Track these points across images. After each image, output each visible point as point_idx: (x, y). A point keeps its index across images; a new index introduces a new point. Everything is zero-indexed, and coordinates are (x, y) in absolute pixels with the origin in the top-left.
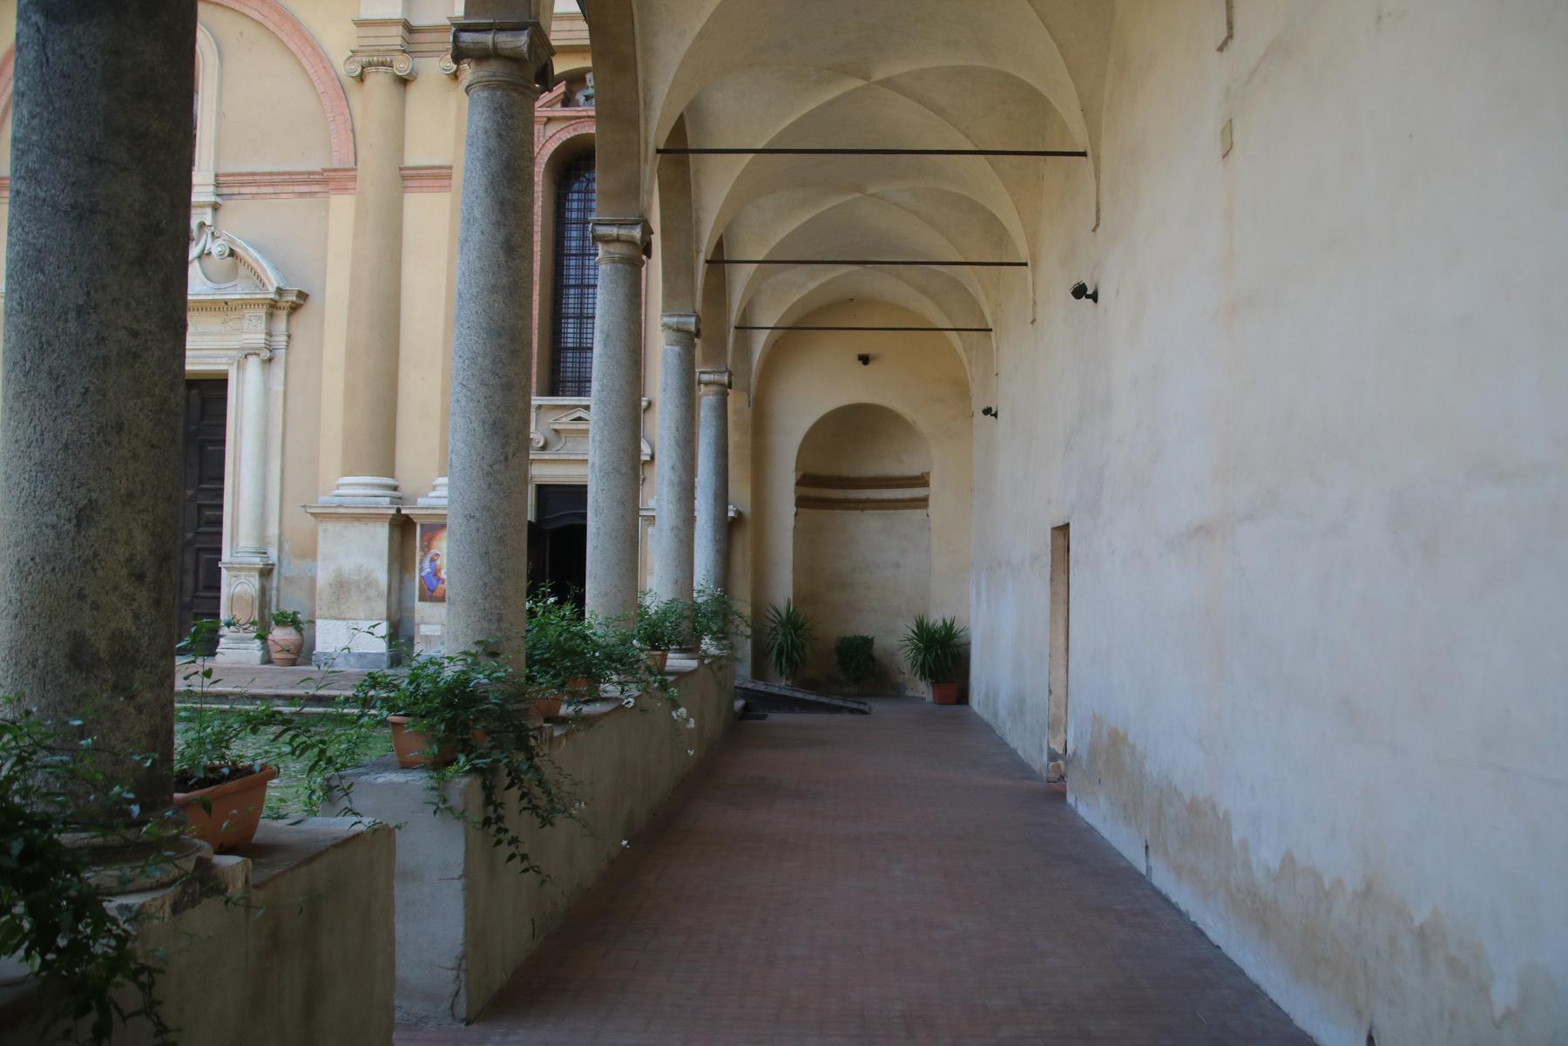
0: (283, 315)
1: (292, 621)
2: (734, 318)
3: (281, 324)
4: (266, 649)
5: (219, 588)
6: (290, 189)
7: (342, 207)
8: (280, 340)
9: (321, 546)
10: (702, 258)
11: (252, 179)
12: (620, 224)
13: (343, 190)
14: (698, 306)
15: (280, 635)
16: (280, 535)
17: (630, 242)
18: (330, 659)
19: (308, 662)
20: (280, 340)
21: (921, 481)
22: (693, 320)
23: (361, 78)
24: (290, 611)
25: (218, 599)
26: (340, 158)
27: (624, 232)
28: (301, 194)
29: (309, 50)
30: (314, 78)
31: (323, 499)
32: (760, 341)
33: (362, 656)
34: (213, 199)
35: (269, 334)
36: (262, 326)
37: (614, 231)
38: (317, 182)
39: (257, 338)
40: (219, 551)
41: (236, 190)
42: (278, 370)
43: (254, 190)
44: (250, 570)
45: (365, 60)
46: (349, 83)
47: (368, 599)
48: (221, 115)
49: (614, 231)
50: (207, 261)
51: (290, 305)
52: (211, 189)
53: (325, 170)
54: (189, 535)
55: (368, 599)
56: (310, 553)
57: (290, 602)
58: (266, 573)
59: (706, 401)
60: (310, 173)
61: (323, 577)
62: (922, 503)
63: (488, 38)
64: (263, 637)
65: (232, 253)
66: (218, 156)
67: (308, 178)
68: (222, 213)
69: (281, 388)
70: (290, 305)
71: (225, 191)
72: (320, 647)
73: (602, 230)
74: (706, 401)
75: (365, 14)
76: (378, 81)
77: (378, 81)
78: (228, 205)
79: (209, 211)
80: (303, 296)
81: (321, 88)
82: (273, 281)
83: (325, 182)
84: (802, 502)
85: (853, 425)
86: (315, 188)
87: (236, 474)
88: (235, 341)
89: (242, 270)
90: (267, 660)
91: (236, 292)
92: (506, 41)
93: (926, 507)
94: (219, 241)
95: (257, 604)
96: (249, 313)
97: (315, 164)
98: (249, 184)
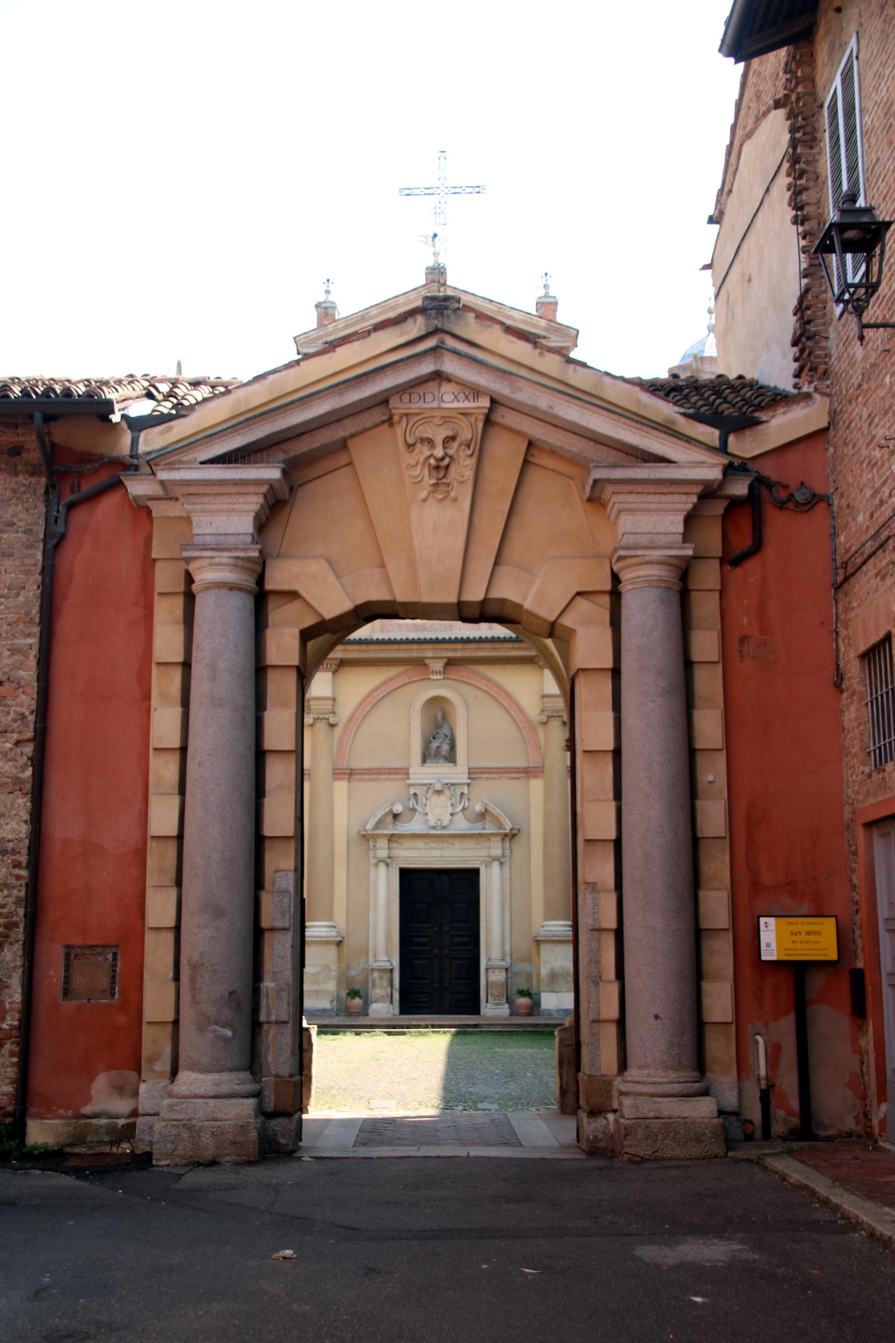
0: (507, 840)
1: (522, 993)
3: (507, 844)
6: (507, 775)
7: (537, 786)
8: (508, 852)
11: (487, 770)
13: (536, 777)
15: (523, 1001)
18: (549, 1013)
23: (544, 724)
28: (513, 778)
29: (514, 707)
30: (517, 720)
33: (566, 1010)
42: (507, 868)
43: (488, 776)
47: (568, 982)
48: (469, 738)
52: (467, 776)
53: (526, 768)
55: (568, 982)
60: (518, 768)
61: (544, 971)
67: (516, 770)
69: (508, 876)
71: (472, 776)
72: (544, 1006)
78: (476, 782)
79: (466, 787)
80: (519, 830)
81: (521, 726)
82: (508, 826)
86: (520, 775)
88: (484, 853)
90: (511, 1015)
96: (493, 839)
97: (521, 763)
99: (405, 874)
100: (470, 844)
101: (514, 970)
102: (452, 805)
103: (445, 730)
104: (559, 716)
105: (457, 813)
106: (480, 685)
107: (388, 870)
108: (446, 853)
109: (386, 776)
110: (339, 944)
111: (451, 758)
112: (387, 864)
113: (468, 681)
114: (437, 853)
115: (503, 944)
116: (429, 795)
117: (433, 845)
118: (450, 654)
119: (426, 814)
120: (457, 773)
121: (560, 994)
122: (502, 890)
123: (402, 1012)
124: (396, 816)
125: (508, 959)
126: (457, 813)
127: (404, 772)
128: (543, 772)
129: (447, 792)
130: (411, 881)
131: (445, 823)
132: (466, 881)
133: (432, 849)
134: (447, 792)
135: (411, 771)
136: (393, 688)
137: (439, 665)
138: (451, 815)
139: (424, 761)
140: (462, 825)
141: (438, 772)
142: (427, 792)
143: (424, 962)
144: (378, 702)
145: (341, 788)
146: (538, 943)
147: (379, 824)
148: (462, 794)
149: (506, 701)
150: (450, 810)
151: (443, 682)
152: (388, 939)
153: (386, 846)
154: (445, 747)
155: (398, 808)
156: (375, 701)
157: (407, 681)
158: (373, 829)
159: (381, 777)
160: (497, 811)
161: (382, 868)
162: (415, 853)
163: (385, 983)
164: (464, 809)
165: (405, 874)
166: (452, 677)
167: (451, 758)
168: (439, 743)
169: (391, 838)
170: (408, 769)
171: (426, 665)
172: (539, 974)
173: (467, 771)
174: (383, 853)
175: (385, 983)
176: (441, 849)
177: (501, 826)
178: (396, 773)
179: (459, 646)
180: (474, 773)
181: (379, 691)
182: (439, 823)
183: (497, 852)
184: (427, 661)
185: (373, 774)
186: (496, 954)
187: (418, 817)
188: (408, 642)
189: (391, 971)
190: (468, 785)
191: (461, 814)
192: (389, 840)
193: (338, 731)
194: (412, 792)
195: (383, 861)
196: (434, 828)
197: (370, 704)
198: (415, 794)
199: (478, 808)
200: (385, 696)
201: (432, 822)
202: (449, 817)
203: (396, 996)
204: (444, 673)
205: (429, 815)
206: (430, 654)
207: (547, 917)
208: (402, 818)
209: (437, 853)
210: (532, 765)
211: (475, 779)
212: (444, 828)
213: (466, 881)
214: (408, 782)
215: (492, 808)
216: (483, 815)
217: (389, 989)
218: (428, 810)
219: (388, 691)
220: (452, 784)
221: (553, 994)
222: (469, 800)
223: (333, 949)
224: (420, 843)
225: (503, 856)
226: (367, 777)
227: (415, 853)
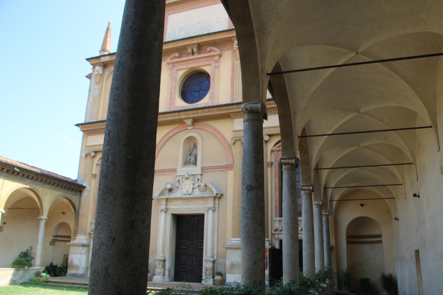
0: (217, 199)
1: (219, 274)
2: (329, 198)
3: (217, 202)
4: (214, 281)
5: (202, 266)
7: (231, 173)
8: (217, 205)
9: (228, 256)
10: (322, 187)
12: (307, 186)
13: (231, 169)
14: (322, 199)
15: (217, 278)
16: (217, 253)
17: (310, 190)
19: (224, 284)
20: (217, 205)
21: (380, 236)
22: (321, 202)
23: (234, 144)
24: (220, 271)
25: (202, 268)
26: (230, 162)
27: (308, 188)
28: (221, 171)
31: (228, 244)
32: (335, 203)
34: (201, 173)
35: (214, 204)
36: (212, 202)
37: (306, 188)
38: (224, 168)
39: (211, 205)
40: (202, 256)
41: (206, 171)
42: (216, 213)
43: (210, 170)
44: (210, 261)
45: (235, 139)
46: (231, 145)
47: (239, 269)
48: (202, 153)
49: (306, 188)
50: (199, 187)
51: (219, 197)
52: (200, 171)
53: (226, 165)
54: (195, 253)
55: (239, 269)
56: (225, 257)
57: (219, 269)
58: (214, 262)
59: (324, 219)
61: (228, 263)
62: (380, 242)
63: (287, 161)
64: (213, 277)
65: (206, 186)
66: (202, 163)
68: (203, 176)
70: (219, 197)
71: (204, 171)
73: (303, 188)
74: (324, 219)
75: (235, 129)
78: (204, 174)
79: (200, 176)
80: (222, 195)
82: (215, 192)
83: (227, 168)
84: (348, 242)
85: (360, 222)
86: (224, 169)
87: (207, 238)
89: (208, 189)
91: (207, 194)
92: (290, 161)
93: (382, 243)
94: (203, 183)
95: (212, 270)
97: (224, 163)
98: (209, 169)
100: (201, 202)
101: (219, 262)
102: (193, 184)
103: (194, 152)
104: (239, 140)
105: (196, 188)
106: (208, 130)
107: (166, 215)
108: (190, 206)
109: (168, 173)
111: (195, 163)
112: (166, 212)
113: (203, 128)
114: (186, 207)
115: (213, 249)
116: (183, 180)
117: (185, 203)
118: (192, 116)
119: (182, 189)
120: (196, 170)
121: (235, 275)
124: (170, 190)
125: (215, 257)
126: (196, 188)
127: (175, 170)
128: (233, 167)
129: (191, 178)
131: (190, 193)
132: (199, 219)
133: (185, 204)
134: (191, 178)
135: (178, 170)
136: (172, 134)
137: (189, 122)
138: (193, 189)
140: (197, 193)
142: (182, 178)
143: (185, 257)
144: (167, 141)
148: (198, 179)
149: (219, 135)
150: (192, 187)
151: (193, 130)
153: (165, 203)
154: (193, 159)
155: (169, 186)
156: (165, 141)
157: (179, 131)
158: (159, 196)
159: (166, 173)
160: (210, 186)
161: (163, 214)
164: (199, 186)
166: (196, 127)
169: (167, 199)
170: (176, 169)
171: (184, 123)
172: (225, 264)
173: (200, 168)
174: (163, 207)
175: (161, 266)
176: (188, 205)
177: (212, 192)
178: (172, 171)
179: (195, 112)
181: (167, 136)
182: (187, 192)
183: (211, 205)
184: (184, 120)
185: (163, 172)
187: (179, 190)
189: (164, 261)
190: (201, 175)
191: (197, 188)
192: (167, 201)
194: (177, 179)
195: (163, 210)
196: (185, 195)
198: (179, 180)
200: (169, 138)
201: (185, 192)
202: (192, 190)
204: (193, 126)
205: (184, 189)
206: (183, 117)
207: (234, 237)
208: (173, 191)
209: (186, 207)
210: (229, 164)
211: (205, 172)
212: (190, 194)
213: (199, 219)
214: (176, 175)
215: (208, 184)
217: (162, 270)
218: (183, 187)
219: (171, 136)
220: (193, 175)
221: (232, 275)
222: (201, 182)
224: (180, 202)
225: (214, 207)
226: (160, 174)
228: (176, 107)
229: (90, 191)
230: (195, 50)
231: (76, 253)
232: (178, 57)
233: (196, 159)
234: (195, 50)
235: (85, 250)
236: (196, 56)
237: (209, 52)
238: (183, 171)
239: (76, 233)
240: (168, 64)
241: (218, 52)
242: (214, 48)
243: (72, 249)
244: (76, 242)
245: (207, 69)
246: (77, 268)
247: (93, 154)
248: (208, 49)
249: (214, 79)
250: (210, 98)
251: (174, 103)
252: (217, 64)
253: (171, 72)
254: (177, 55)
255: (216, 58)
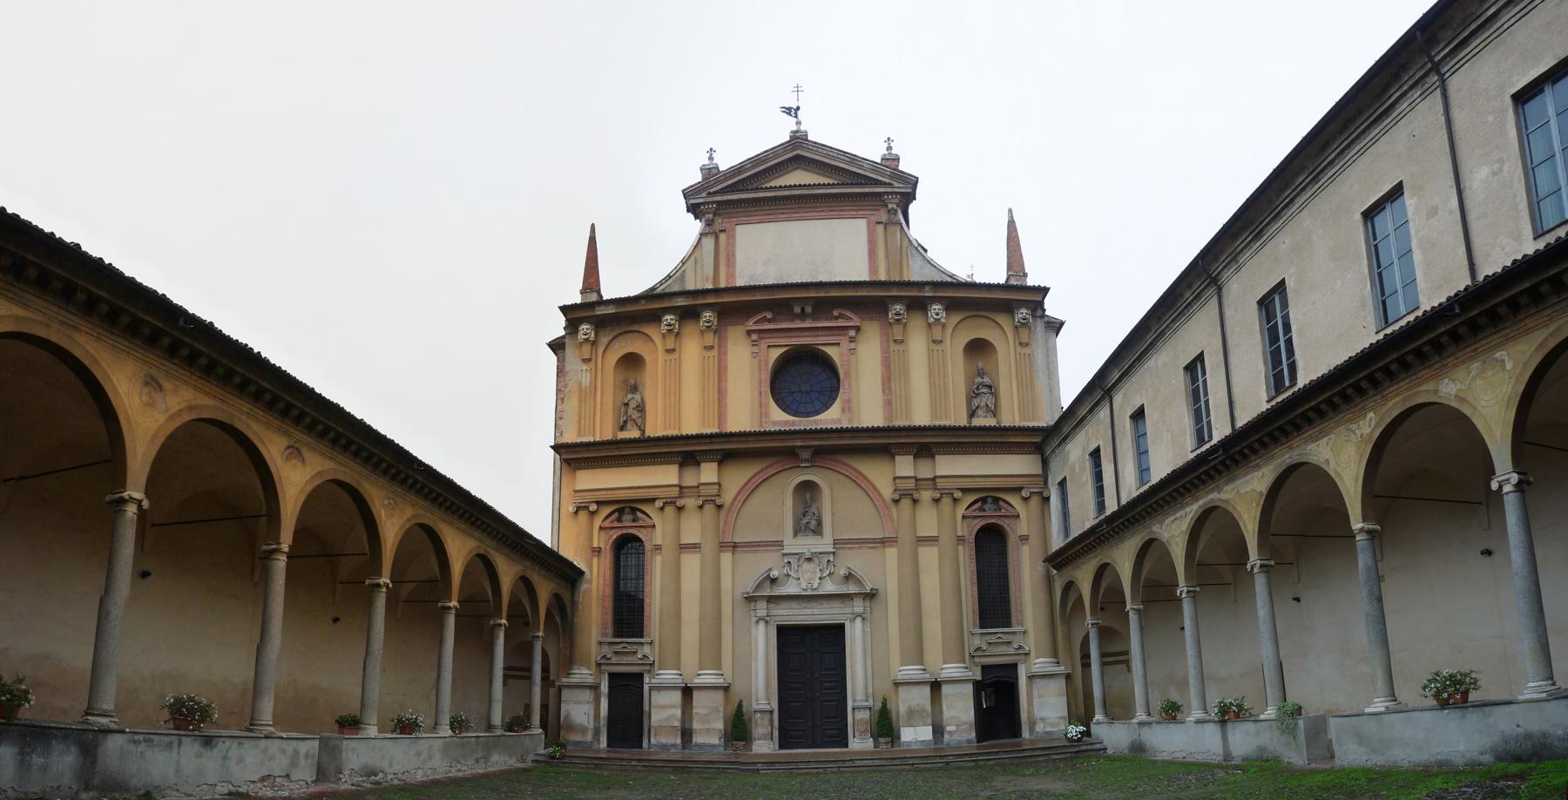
7: (891, 553)
23: (896, 502)
61: (902, 709)
67: (874, 541)
76: (906, 503)
77: (906, 503)
99: (782, 630)
108: (816, 611)
110: (726, 689)
111: (818, 531)
114: (809, 611)
120: (824, 544)
122: (864, 641)
123: (781, 747)
124: (774, 581)
127: (779, 544)
130: (788, 636)
137: (806, 455)
139: (795, 534)
140: (830, 587)
141: (809, 544)
145: (726, 557)
146: (897, 684)
147: (758, 587)
152: (768, 685)
154: (813, 522)
155: (775, 574)
161: (762, 625)
162: (790, 612)
163: (767, 723)
164: (831, 574)
165: (782, 630)
167: (818, 531)
168: (807, 523)
169: (771, 599)
174: (762, 613)
180: (836, 542)
183: (861, 610)
186: (860, 696)
188: (780, 433)
193: (723, 513)
197: (750, 490)
199: (843, 572)
203: (776, 734)
213: (836, 632)
216: (849, 577)
223: (720, 695)
224: (794, 604)
227: (790, 612)
228: (774, 423)
229: (590, 581)
230: (809, 310)
231: (579, 702)
232: (769, 321)
233: (820, 523)
234: (809, 310)
235: (587, 695)
236: (808, 324)
237: (836, 318)
238: (794, 545)
239: (569, 661)
240: (749, 333)
241: (856, 321)
242: (849, 314)
243: (566, 694)
244: (574, 680)
245: (830, 351)
246: (583, 730)
247: (593, 507)
248: (836, 313)
249: (847, 374)
250: (843, 411)
251: (767, 414)
252: (853, 345)
253: (755, 349)
254: (769, 316)
255: (852, 333)
